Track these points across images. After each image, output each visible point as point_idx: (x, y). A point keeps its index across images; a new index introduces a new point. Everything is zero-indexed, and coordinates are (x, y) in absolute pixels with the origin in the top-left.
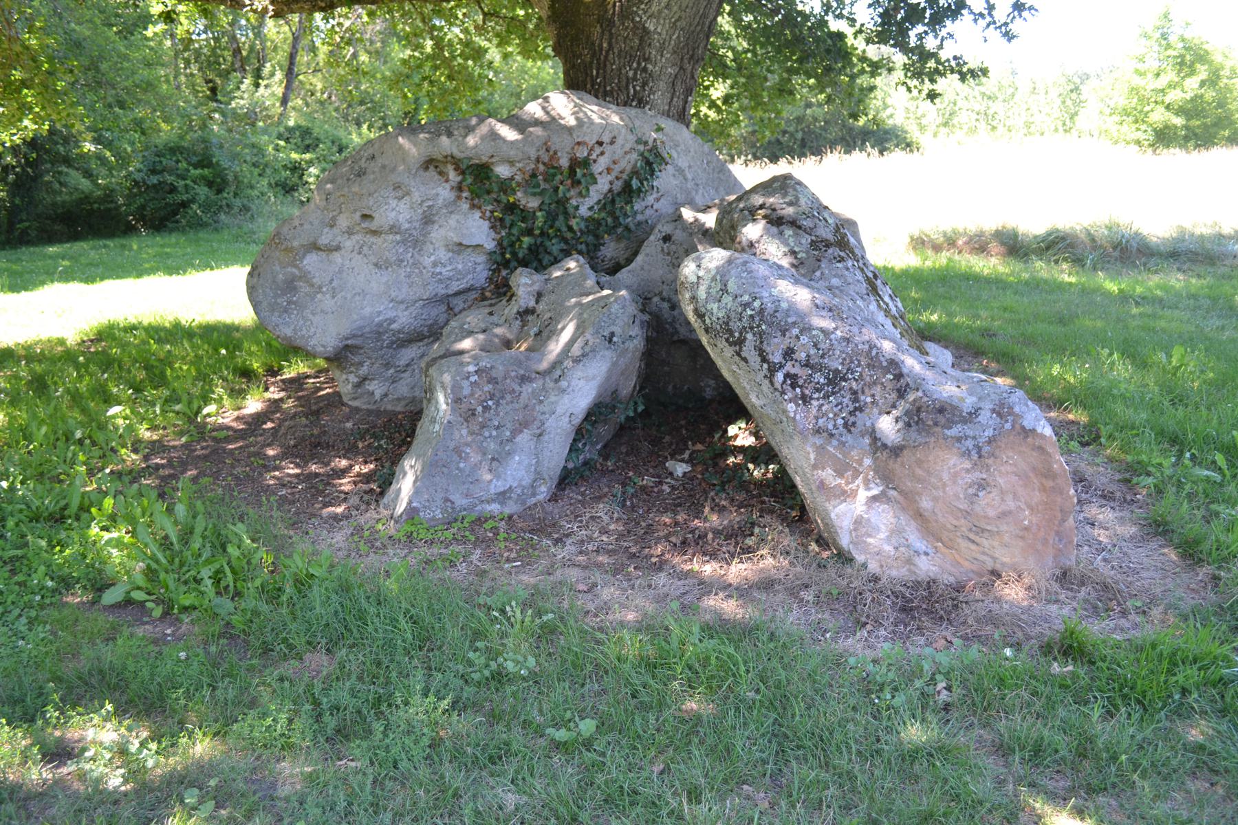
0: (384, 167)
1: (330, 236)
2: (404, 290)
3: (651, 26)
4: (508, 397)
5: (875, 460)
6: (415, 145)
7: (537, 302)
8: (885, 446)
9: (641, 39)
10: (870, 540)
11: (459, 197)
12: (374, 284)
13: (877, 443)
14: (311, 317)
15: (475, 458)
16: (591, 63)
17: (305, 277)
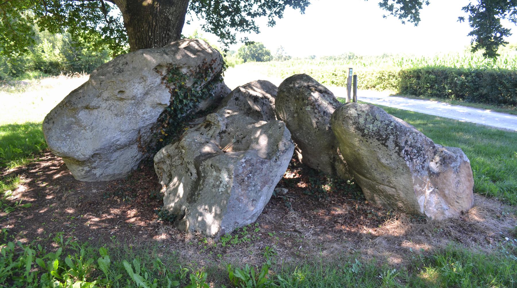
0: (134, 68)
1: (96, 102)
2: (126, 126)
3: (170, 17)
4: (258, 171)
5: (431, 179)
6: (154, 58)
7: (226, 128)
8: (434, 173)
9: (167, 23)
10: (430, 208)
11: (162, 83)
12: (113, 124)
13: (431, 174)
14: (78, 141)
15: (245, 201)
16: (149, 30)
17: (78, 122)
